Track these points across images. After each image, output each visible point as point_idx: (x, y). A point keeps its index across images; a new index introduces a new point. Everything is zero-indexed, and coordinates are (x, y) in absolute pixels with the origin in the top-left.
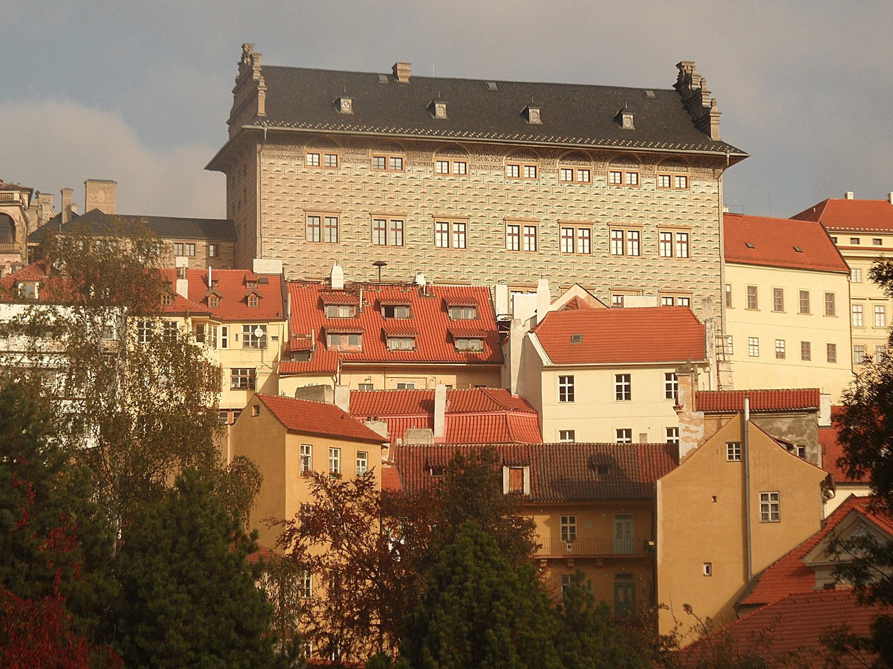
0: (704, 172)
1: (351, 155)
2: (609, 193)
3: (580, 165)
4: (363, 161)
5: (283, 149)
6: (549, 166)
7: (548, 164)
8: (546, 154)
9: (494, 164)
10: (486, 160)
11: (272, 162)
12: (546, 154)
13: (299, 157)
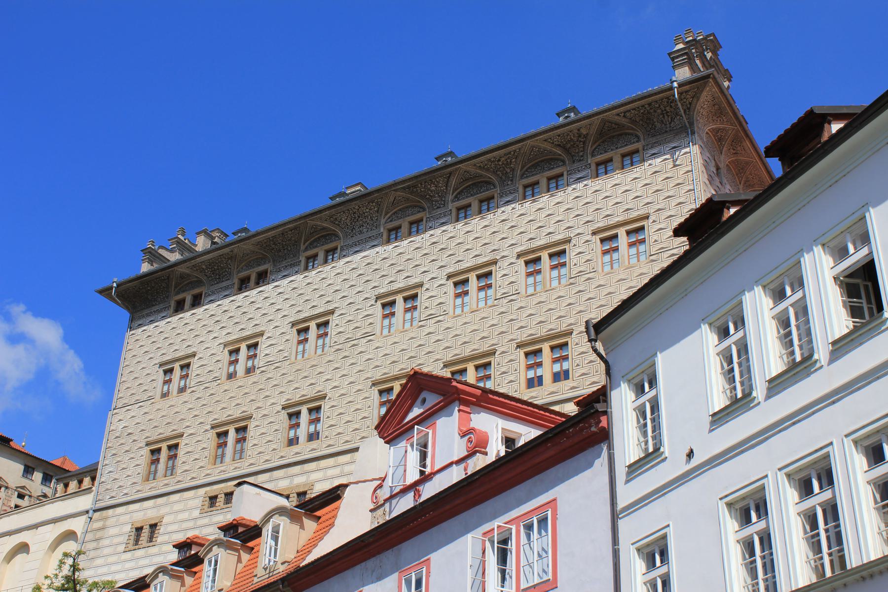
0: (666, 132)
1: (216, 286)
2: (521, 212)
3: (481, 193)
4: (227, 288)
5: (153, 305)
6: (438, 210)
7: (438, 208)
8: (430, 196)
9: (370, 234)
10: (361, 232)
11: (140, 323)
12: (430, 196)
13: (166, 308)
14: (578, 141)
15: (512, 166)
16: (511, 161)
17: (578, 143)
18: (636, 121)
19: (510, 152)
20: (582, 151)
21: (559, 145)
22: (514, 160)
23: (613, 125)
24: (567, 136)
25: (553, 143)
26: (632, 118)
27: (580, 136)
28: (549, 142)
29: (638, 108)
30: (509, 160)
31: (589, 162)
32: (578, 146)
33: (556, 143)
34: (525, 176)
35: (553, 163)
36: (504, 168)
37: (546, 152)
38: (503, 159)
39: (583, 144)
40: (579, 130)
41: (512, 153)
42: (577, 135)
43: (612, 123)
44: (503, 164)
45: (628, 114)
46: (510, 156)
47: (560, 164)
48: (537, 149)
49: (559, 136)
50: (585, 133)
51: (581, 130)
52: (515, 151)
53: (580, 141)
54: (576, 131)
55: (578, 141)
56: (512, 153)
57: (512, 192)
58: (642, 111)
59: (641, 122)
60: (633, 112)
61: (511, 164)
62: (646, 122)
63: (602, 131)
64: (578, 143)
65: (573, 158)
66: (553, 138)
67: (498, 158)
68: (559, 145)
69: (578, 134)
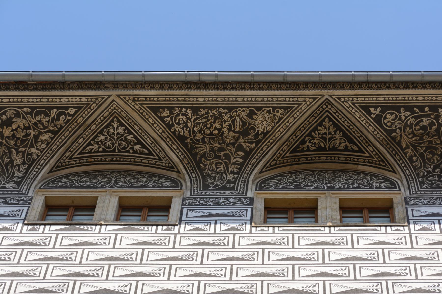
14: (233, 144)
15: (33, 150)
16: (36, 137)
17: (233, 150)
18: (399, 144)
19: (50, 109)
20: (233, 172)
21: (181, 139)
22: (45, 137)
23: (339, 135)
24: (216, 118)
25: (170, 126)
26: (394, 131)
27: (244, 133)
28: (162, 119)
29: (421, 108)
30: (33, 132)
31: (250, 194)
32: (227, 156)
33: (177, 128)
34: (60, 184)
35: (144, 180)
36: (9, 148)
37: (137, 147)
38: (20, 122)
39: (244, 158)
40: (251, 114)
41: (54, 112)
42: (238, 128)
43: (338, 128)
44: (14, 136)
45: (390, 118)
46: (44, 120)
47: (166, 184)
48: (120, 130)
49: (195, 110)
50: (261, 129)
51: (258, 117)
52: (62, 110)
53: (240, 148)
54: (242, 114)
55: (233, 144)
56: (54, 112)
57: (12, 202)
58: (425, 122)
59: (409, 152)
60: (404, 113)
61: (32, 146)
62: (422, 155)
63: (303, 142)
64: (233, 150)
65: (204, 181)
66: (177, 110)
67: (10, 113)
68: (181, 139)
69: (244, 123)
